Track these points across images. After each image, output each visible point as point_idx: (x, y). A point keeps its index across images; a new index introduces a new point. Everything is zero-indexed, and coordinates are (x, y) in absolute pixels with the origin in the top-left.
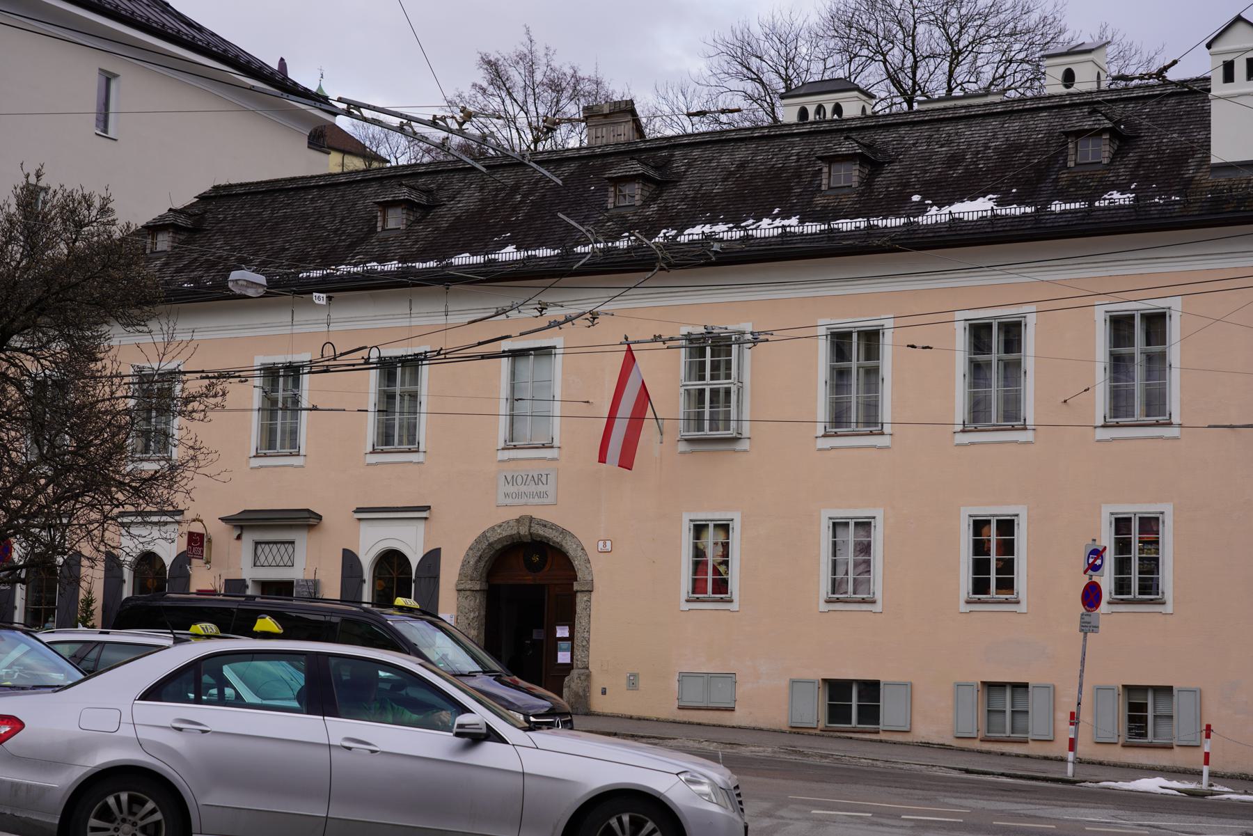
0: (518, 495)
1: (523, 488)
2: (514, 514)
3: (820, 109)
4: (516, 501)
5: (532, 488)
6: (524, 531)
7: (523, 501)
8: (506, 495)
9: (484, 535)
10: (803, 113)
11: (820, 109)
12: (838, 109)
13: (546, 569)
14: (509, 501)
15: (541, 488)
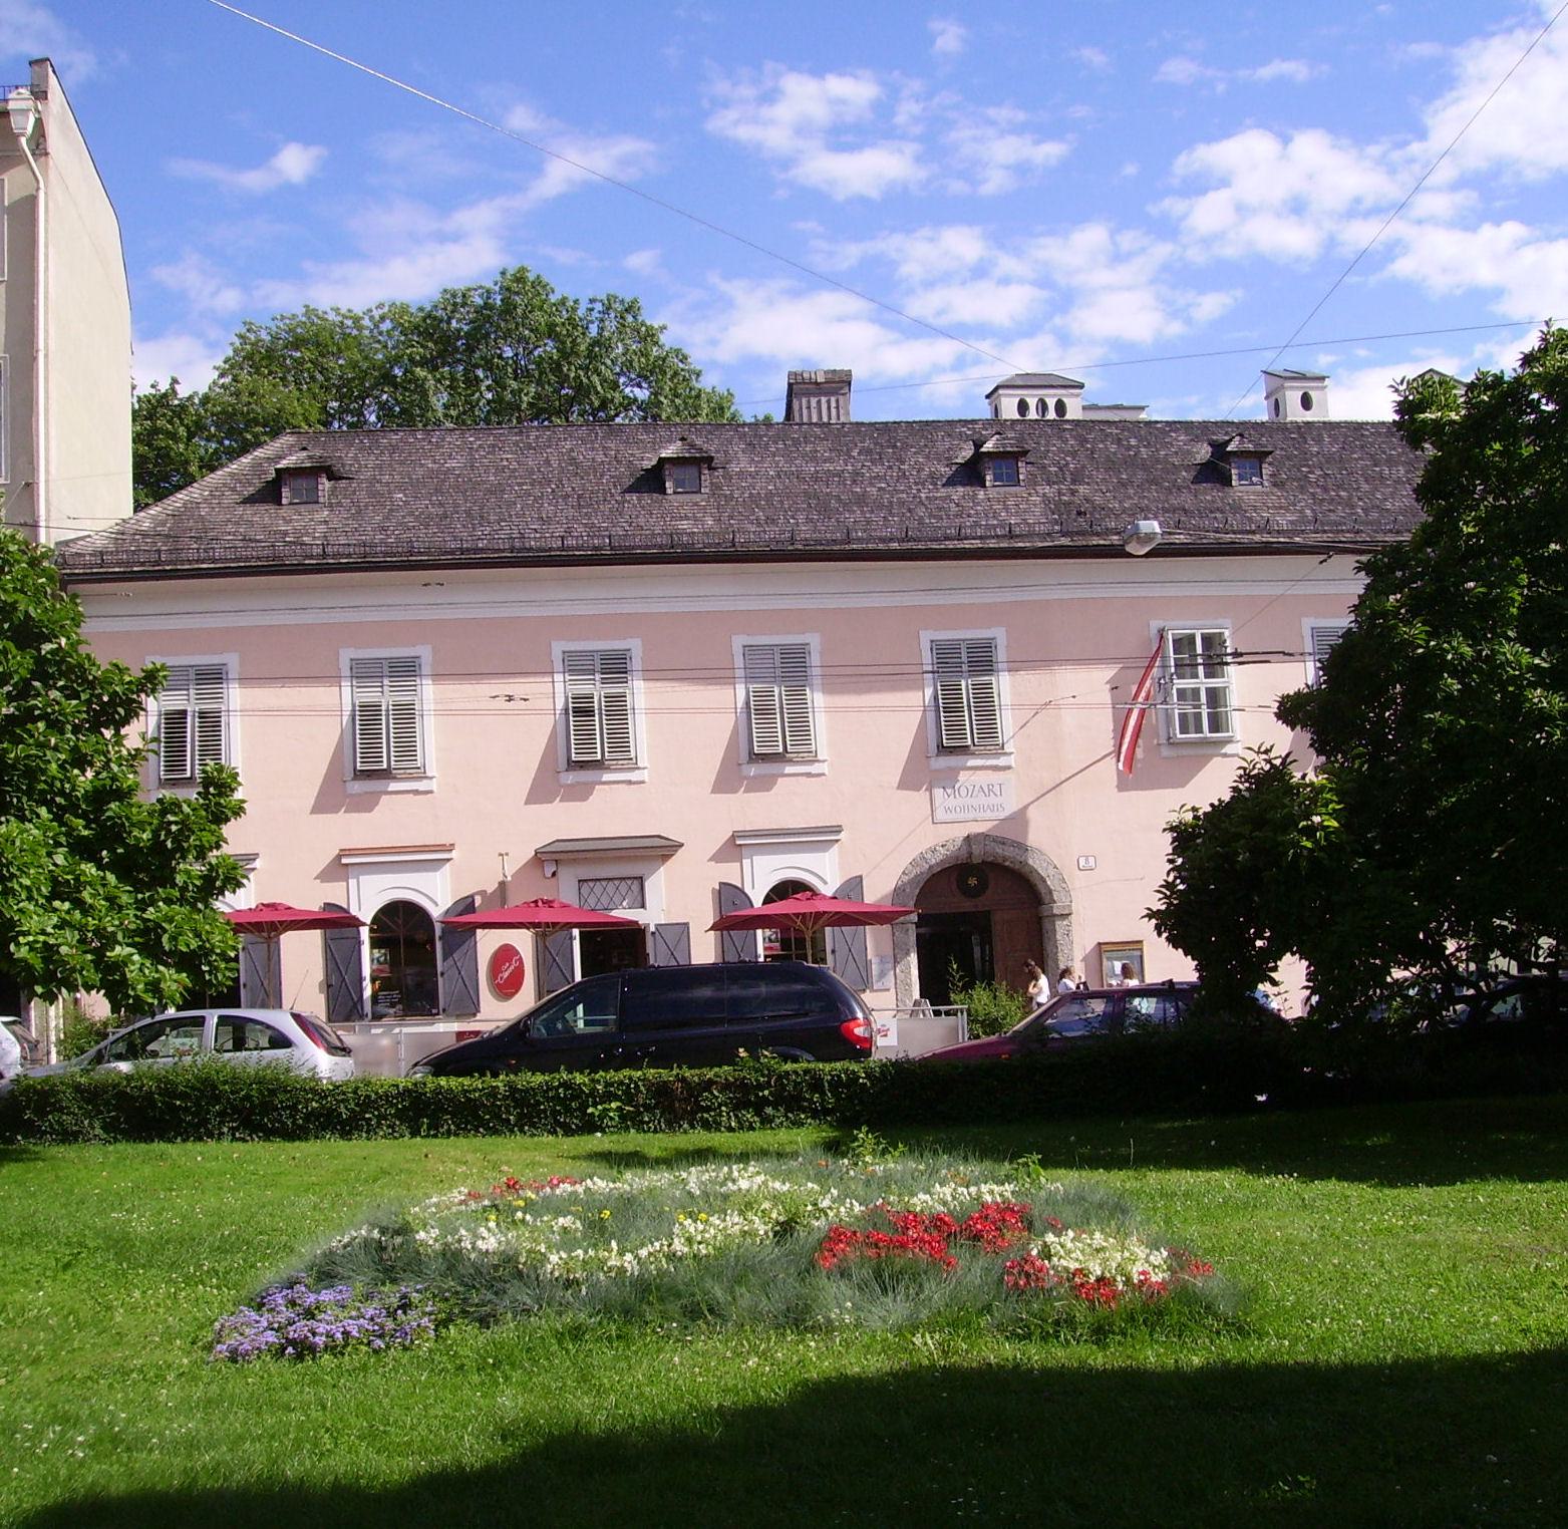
0: (963, 809)
1: (969, 801)
2: (960, 832)
3: (1043, 406)
4: (961, 816)
5: (982, 800)
6: (977, 850)
7: (971, 816)
8: (947, 810)
9: (922, 856)
10: (1023, 407)
11: (1043, 406)
12: (1061, 407)
13: (989, 892)
14: (950, 817)
15: (992, 800)
